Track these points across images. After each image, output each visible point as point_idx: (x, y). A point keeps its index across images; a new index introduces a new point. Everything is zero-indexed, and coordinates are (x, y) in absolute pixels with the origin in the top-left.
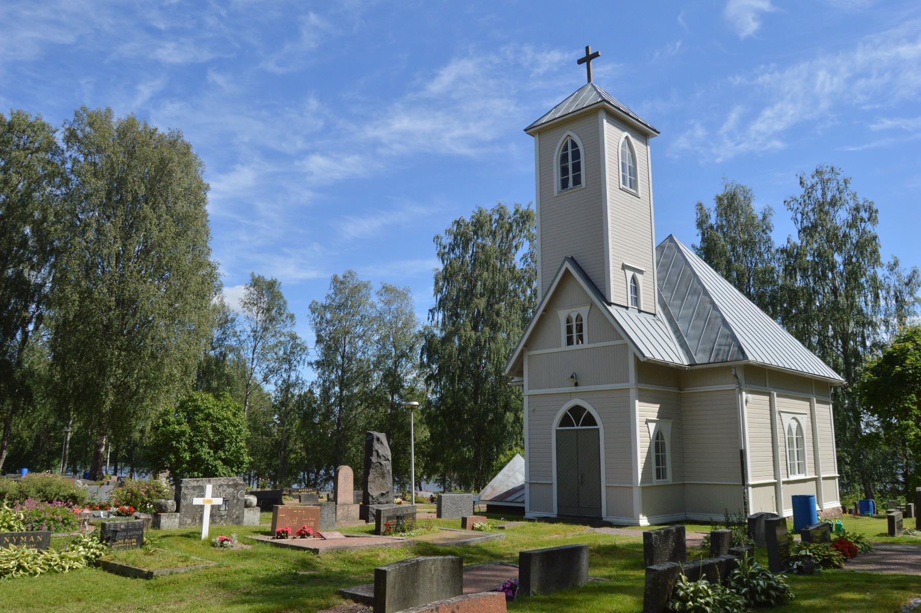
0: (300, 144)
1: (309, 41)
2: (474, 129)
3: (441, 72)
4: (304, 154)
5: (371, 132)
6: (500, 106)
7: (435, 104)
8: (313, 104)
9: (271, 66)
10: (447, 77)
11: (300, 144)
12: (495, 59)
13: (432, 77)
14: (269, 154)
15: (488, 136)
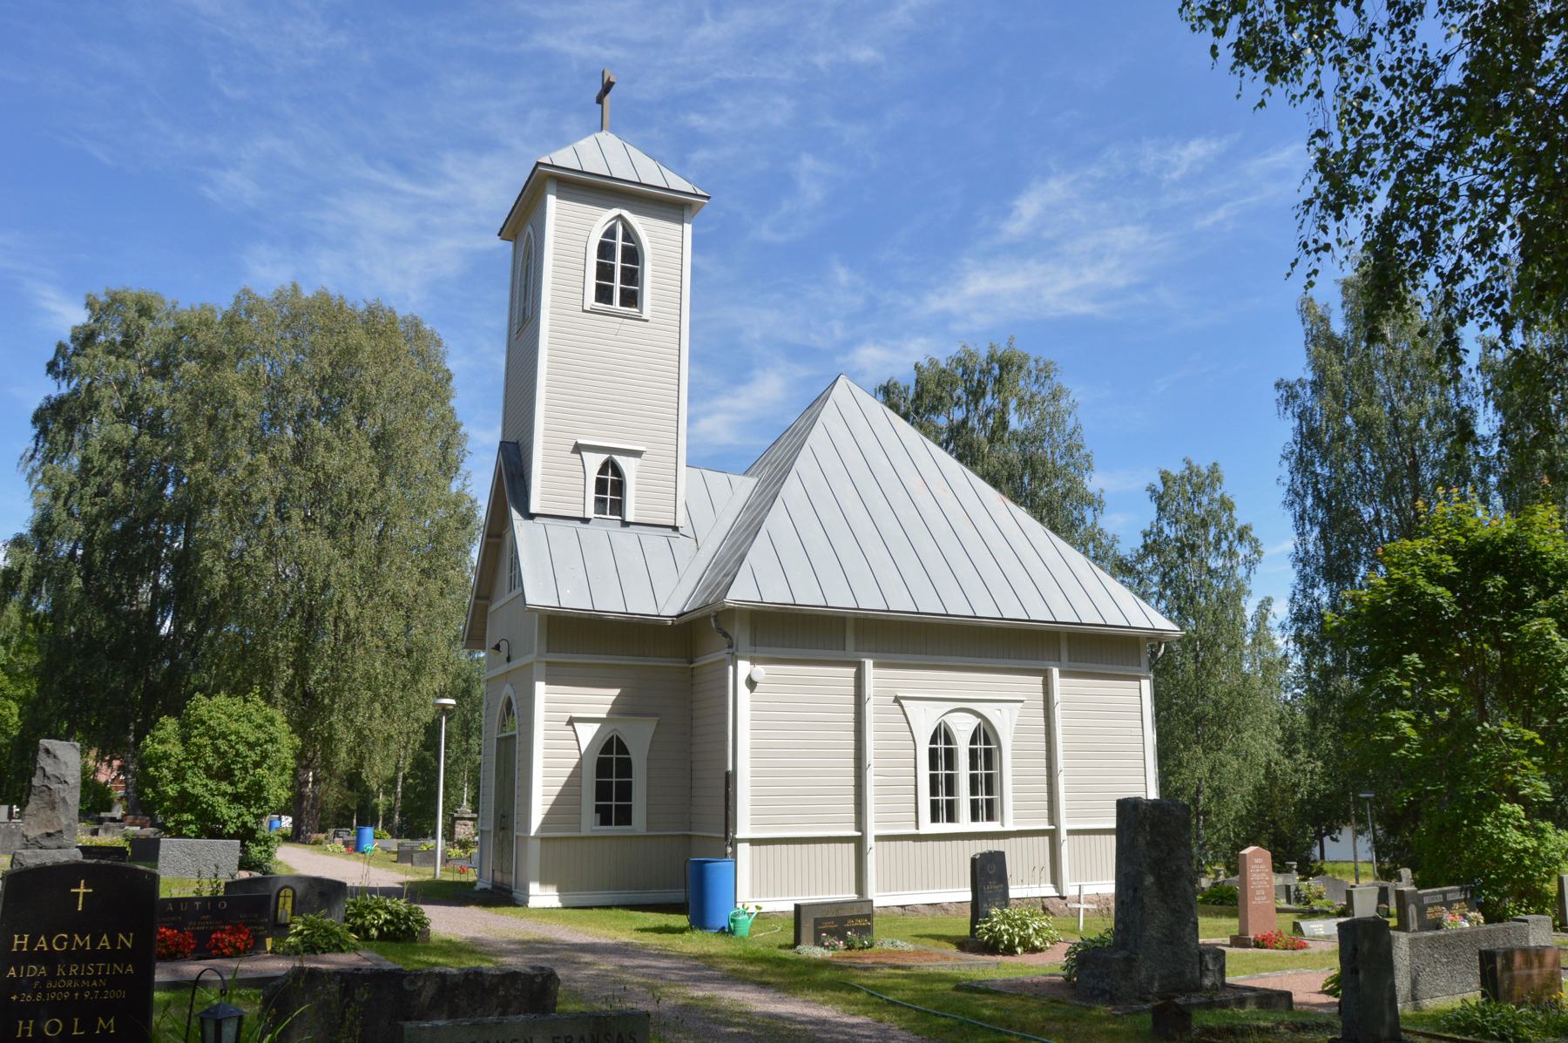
0: (839, 331)
1: (813, 193)
2: (1091, 276)
3: (1017, 203)
4: (848, 345)
5: (935, 303)
6: (1127, 236)
7: (1020, 250)
8: (843, 275)
9: (765, 233)
10: (1029, 207)
11: (839, 331)
12: (1097, 172)
13: (1007, 213)
14: (799, 353)
15: (1120, 281)
